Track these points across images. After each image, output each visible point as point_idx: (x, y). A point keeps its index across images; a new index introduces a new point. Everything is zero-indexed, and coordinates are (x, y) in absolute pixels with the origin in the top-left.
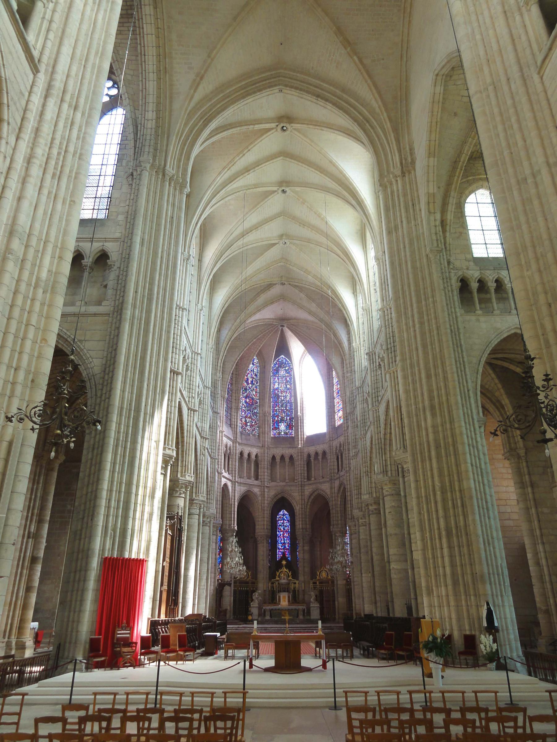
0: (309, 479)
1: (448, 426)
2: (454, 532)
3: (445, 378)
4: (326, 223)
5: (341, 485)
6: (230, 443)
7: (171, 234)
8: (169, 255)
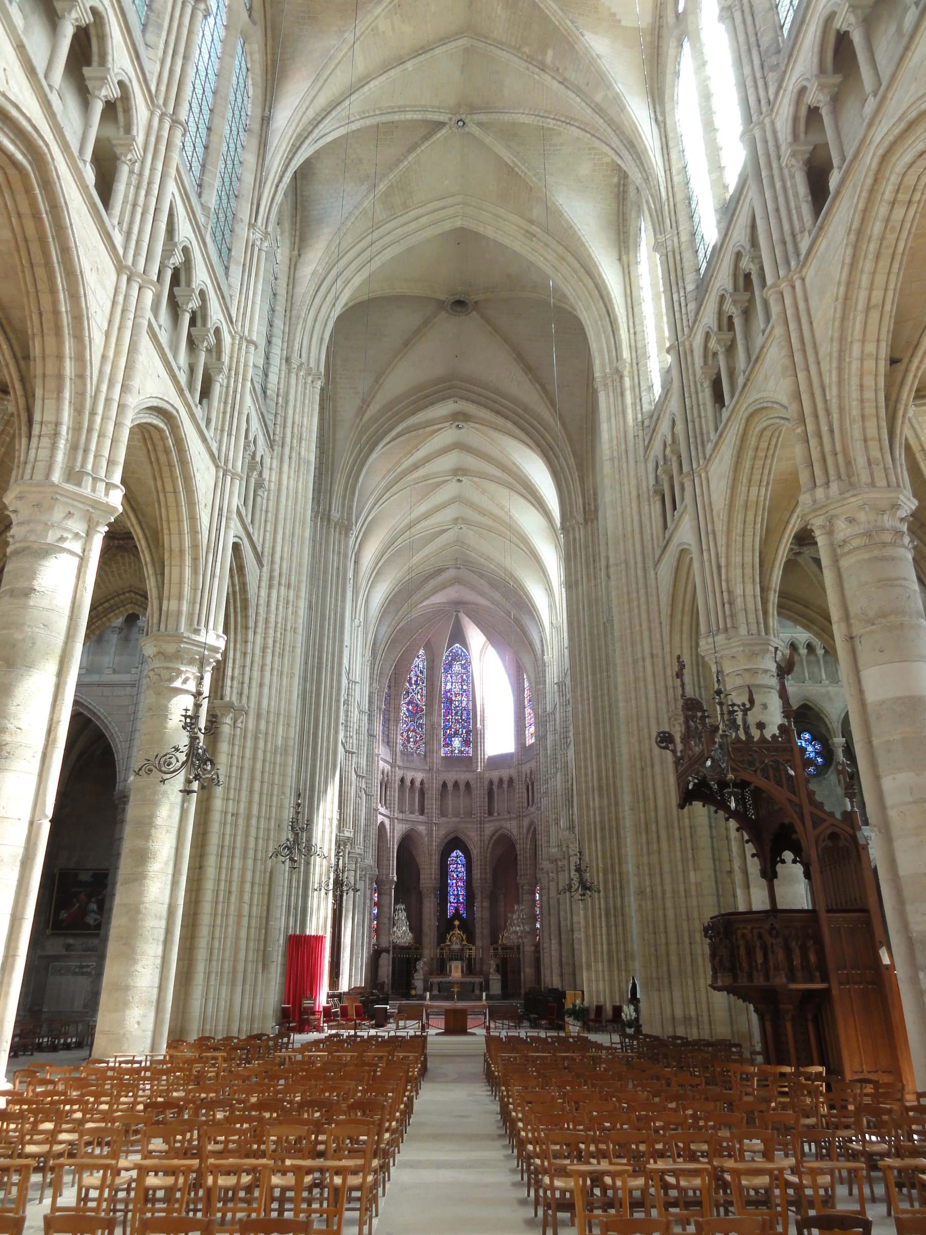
0: (490, 813)
4: (510, 517)
5: (531, 823)
6: (387, 767)
8: (336, 614)
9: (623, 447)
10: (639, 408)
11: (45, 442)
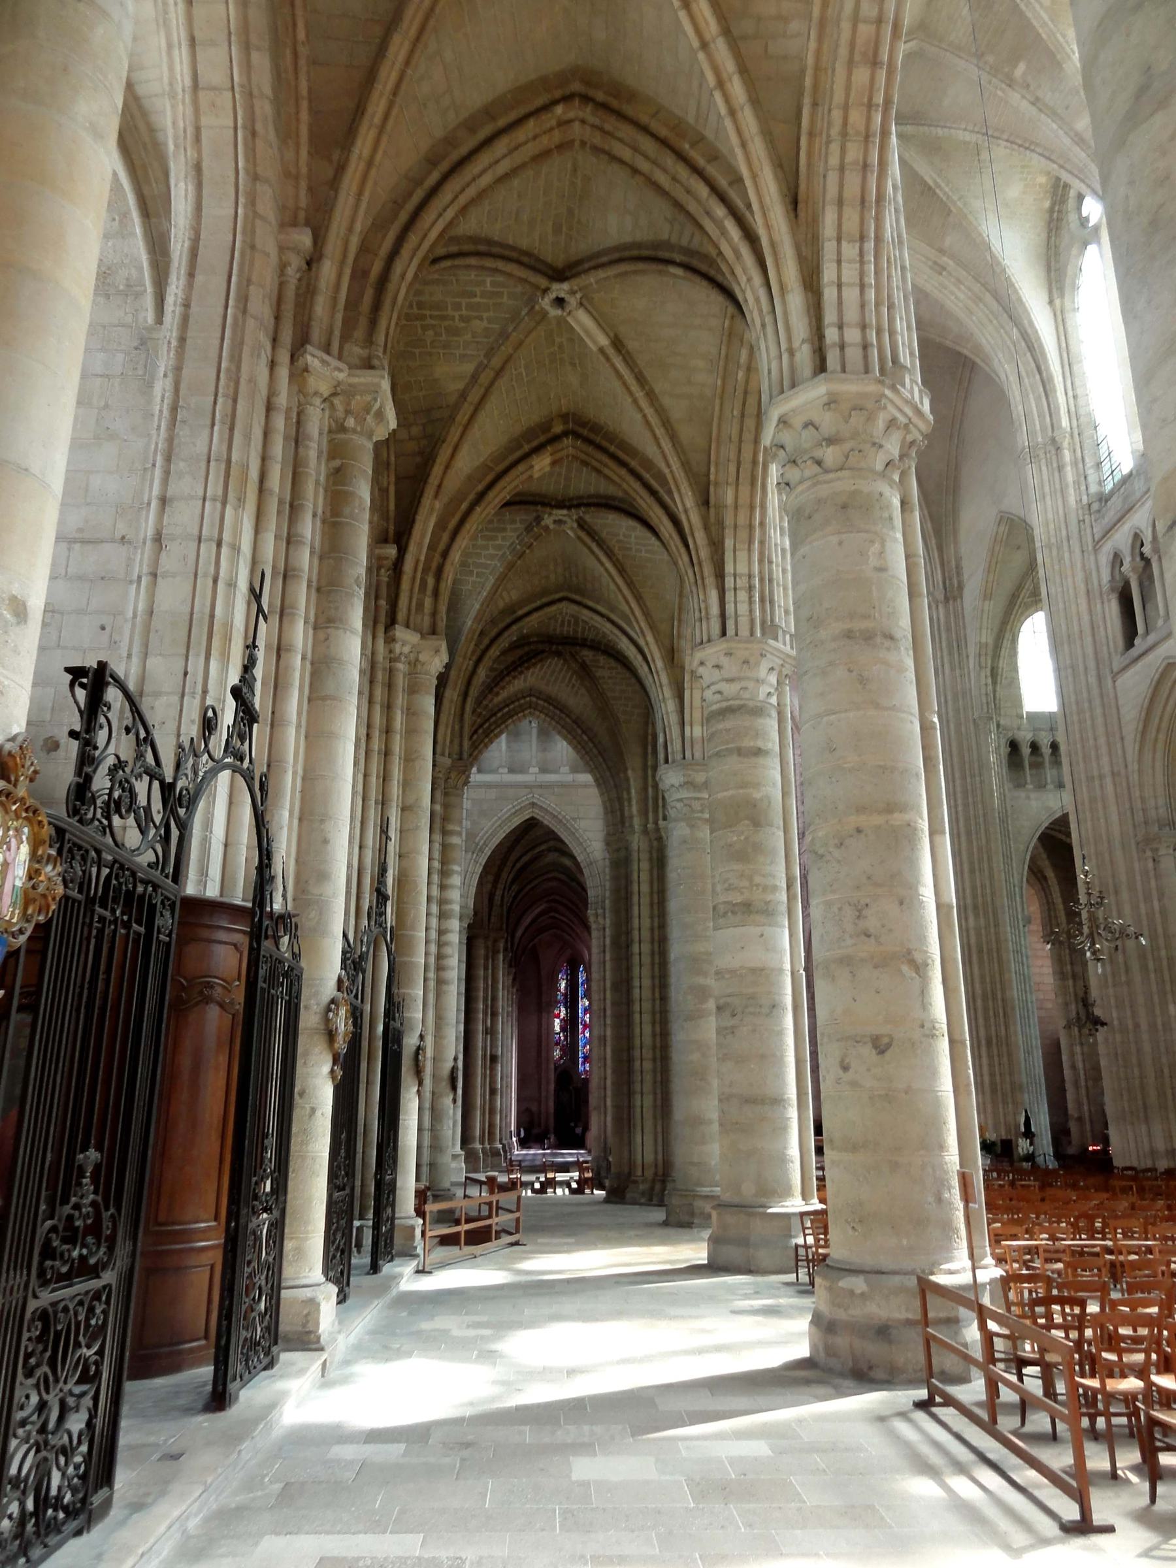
1: (992, 930)
2: (994, 1041)
3: (991, 877)
9: (1064, 533)
10: (1083, 488)
11: (742, 596)
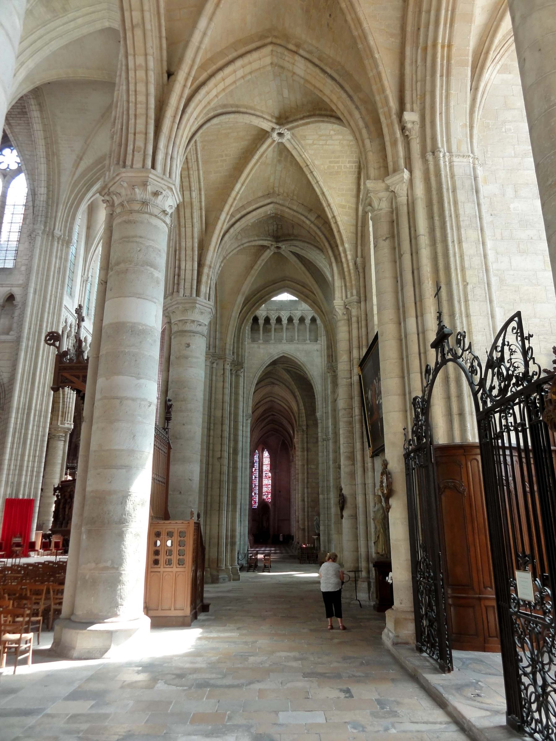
7: (58, 280)
8: (56, 297)
